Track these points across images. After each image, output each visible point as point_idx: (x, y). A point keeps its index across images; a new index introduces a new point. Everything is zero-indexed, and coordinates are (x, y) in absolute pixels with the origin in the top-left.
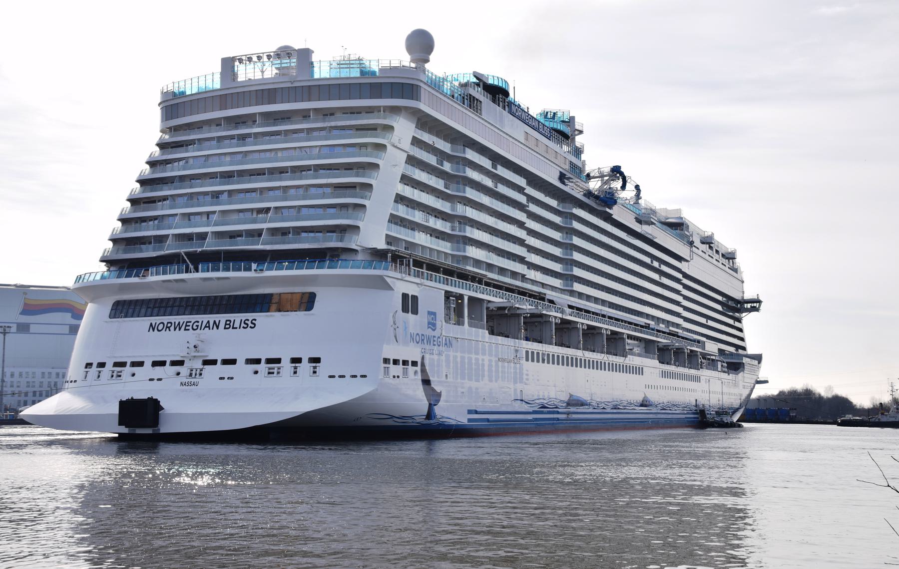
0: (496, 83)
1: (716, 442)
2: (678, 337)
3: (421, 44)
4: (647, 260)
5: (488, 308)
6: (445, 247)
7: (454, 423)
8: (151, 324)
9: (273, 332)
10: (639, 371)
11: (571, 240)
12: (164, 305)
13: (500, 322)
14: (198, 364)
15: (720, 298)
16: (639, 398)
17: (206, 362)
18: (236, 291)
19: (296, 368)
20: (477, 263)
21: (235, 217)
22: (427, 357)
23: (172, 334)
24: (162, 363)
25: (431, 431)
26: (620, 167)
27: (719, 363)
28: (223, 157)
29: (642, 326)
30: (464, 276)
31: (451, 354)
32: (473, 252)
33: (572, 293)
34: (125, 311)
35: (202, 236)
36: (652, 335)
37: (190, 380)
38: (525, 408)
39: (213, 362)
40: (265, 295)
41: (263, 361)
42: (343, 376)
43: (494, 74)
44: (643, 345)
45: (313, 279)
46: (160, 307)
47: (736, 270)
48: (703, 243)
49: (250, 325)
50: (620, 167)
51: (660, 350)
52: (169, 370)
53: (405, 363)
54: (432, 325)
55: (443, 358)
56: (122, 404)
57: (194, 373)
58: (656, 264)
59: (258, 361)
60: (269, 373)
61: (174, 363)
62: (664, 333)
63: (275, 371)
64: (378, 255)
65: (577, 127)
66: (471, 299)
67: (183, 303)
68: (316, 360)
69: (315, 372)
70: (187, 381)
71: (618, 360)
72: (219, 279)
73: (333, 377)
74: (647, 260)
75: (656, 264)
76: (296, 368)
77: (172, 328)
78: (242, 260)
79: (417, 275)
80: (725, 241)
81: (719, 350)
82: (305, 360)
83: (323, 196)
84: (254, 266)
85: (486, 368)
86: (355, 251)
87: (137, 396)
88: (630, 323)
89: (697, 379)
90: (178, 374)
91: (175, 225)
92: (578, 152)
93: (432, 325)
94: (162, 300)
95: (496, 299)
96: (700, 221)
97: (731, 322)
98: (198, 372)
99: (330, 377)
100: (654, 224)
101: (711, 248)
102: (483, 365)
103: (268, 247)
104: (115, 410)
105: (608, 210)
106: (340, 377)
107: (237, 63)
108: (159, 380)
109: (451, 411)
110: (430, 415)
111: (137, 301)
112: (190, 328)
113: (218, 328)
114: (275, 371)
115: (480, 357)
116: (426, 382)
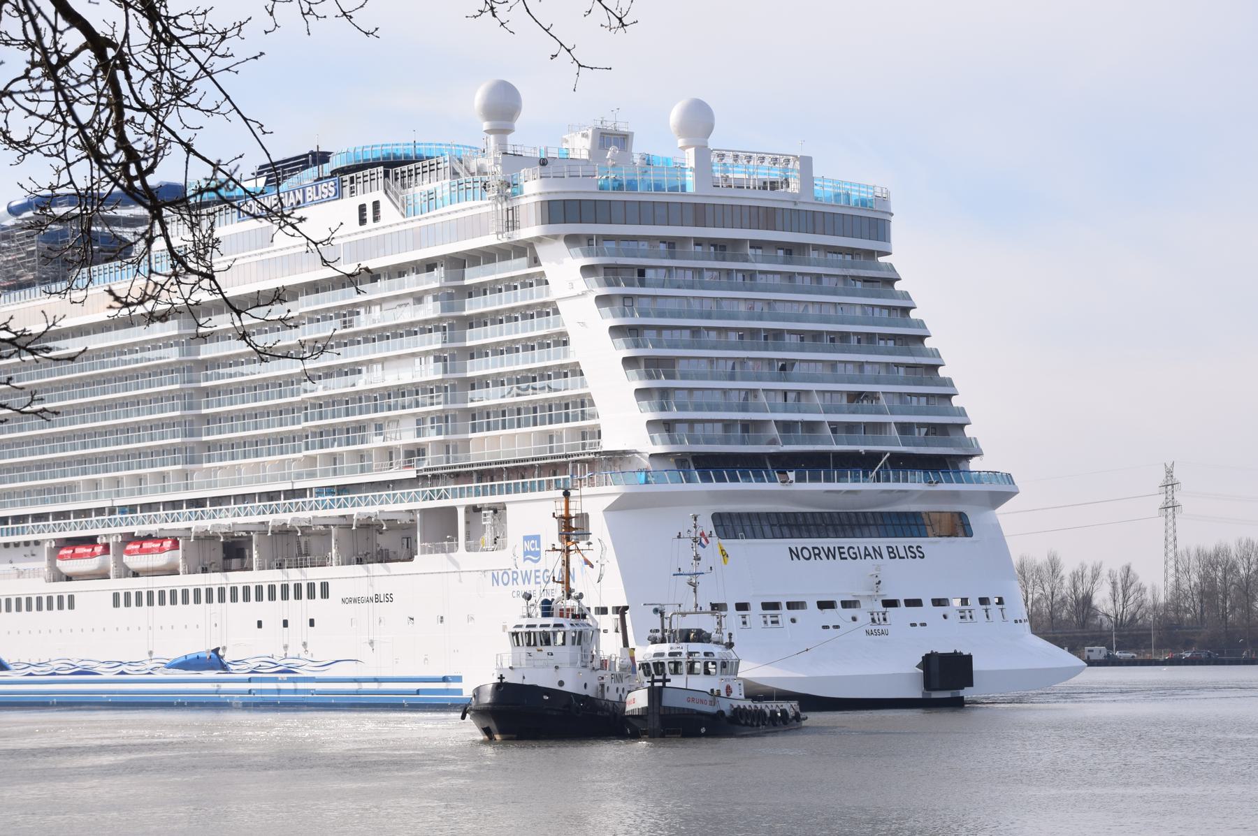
8: (791, 550)
18: (878, 506)
23: (823, 564)
34: (738, 529)
35: (811, 427)
45: (955, 495)
52: (838, 615)
56: (969, 657)
61: (845, 604)
63: (968, 614)
77: (822, 555)
94: (785, 514)
98: (881, 617)
111: (749, 515)
114: (968, 614)
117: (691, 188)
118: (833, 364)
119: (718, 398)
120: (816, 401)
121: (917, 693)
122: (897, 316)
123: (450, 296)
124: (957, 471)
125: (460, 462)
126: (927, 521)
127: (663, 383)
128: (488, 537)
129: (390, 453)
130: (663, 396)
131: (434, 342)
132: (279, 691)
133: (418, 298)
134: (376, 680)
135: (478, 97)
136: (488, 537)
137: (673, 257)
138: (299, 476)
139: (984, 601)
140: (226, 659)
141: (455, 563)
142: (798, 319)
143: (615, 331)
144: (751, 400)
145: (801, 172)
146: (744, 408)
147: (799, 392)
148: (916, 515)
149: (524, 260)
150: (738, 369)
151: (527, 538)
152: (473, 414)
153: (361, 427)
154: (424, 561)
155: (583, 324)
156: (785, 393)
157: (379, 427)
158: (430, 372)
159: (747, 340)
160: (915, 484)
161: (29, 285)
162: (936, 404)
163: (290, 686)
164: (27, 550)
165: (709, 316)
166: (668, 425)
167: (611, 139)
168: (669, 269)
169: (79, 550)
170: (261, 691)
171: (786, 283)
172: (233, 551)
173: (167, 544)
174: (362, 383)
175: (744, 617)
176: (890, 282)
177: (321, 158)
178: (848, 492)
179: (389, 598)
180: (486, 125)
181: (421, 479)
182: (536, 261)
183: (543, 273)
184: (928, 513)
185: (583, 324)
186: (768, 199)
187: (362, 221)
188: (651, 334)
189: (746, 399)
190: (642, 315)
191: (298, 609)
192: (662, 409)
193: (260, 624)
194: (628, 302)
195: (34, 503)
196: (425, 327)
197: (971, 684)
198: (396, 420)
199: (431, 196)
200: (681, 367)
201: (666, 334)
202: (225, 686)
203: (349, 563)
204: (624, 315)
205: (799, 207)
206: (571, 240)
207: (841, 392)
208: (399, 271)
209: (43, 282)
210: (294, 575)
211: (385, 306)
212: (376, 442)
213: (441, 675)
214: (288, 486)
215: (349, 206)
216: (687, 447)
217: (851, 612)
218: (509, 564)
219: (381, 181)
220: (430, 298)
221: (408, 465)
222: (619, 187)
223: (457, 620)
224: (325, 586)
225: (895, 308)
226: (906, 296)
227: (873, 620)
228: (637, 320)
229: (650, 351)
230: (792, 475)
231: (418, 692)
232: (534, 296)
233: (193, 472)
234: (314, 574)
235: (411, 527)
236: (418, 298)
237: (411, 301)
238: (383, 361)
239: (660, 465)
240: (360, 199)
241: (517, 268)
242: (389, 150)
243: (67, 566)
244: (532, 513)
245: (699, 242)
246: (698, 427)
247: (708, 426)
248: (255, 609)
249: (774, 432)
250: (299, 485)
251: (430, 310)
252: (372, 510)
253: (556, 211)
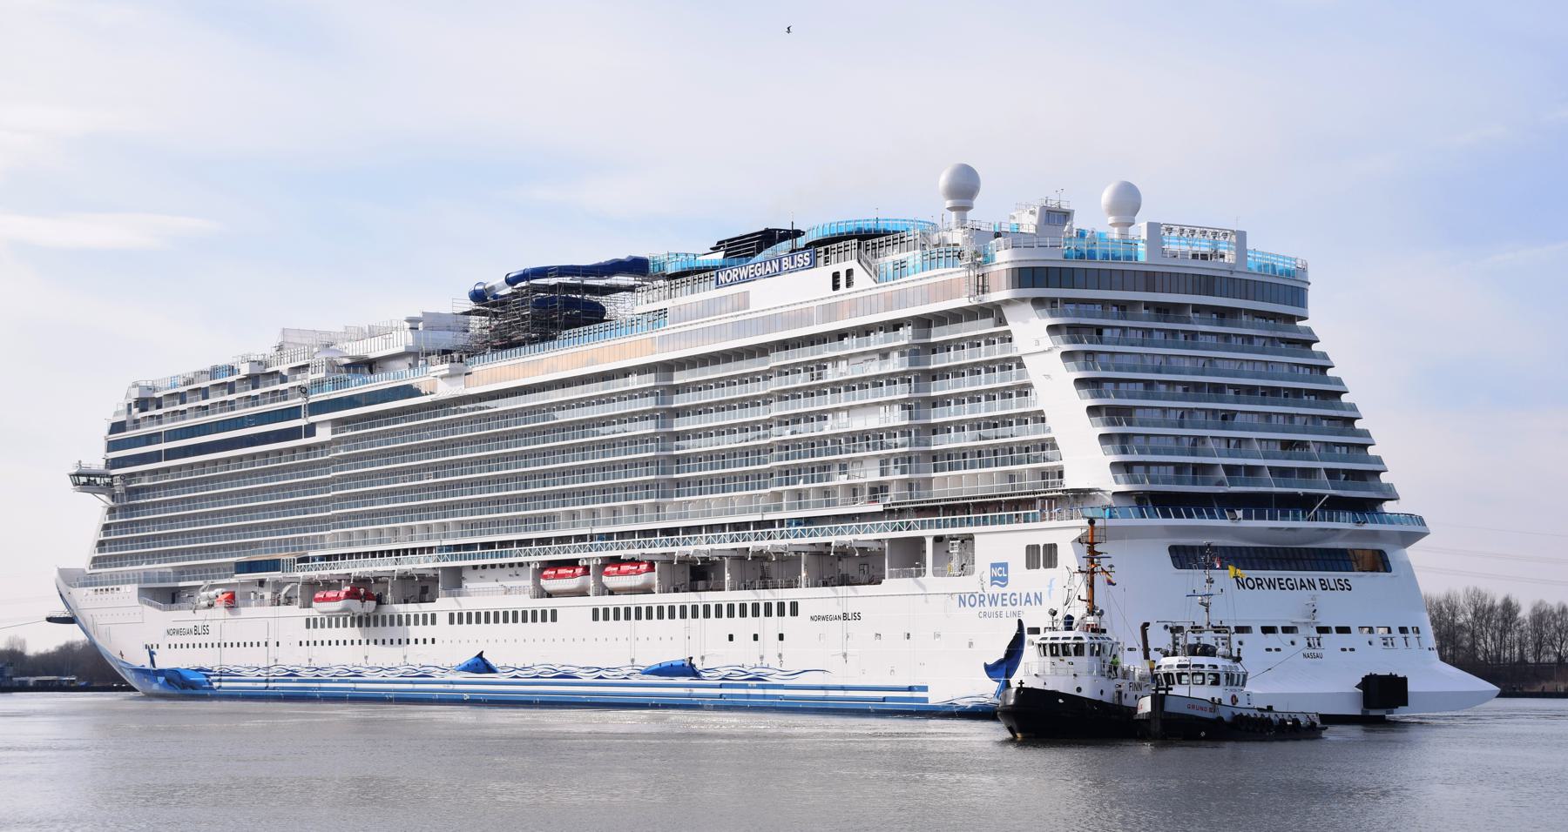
14: (1315, 634)
17: (1323, 630)
35: (1252, 471)
45: (1375, 534)
56: (1405, 680)
61: (1286, 630)
117: (1142, 258)
118: (1268, 415)
119: (1171, 443)
120: (1254, 446)
121: (1356, 710)
122: (1316, 373)
123: (917, 352)
124: (1374, 511)
125: (923, 498)
127: (1124, 429)
128: (955, 564)
129: (854, 490)
130: (1122, 442)
131: (901, 392)
132: (748, 696)
133: (884, 354)
134: (843, 688)
135: (943, 180)
136: (955, 564)
137: (1125, 318)
138: (767, 509)
139: (1403, 630)
140: (699, 667)
141: (922, 586)
142: (1236, 375)
143: (1079, 382)
144: (1199, 446)
145: (1237, 244)
146: (1194, 454)
147: (1239, 440)
148: (1343, 551)
149: (991, 320)
150: (1186, 418)
151: (994, 566)
152: (934, 456)
153: (825, 467)
154: (890, 584)
155: (1048, 376)
156: (1228, 440)
157: (843, 467)
158: (896, 418)
159: (1191, 393)
160: (1345, 524)
161: (520, 344)
162: (1353, 452)
163: (760, 692)
164: (512, 571)
165: (1159, 371)
166: (1127, 467)
167: (1055, 217)
168: (1124, 329)
169: (561, 571)
170: (732, 696)
171: (1221, 342)
172: (700, 574)
173: (644, 567)
174: (829, 428)
176: (1308, 344)
177: (798, 233)
179: (857, 616)
180: (949, 203)
181: (889, 513)
182: (1001, 321)
183: (1009, 332)
184: (1353, 550)
185: (1048, 376)
186: (1200, 268)
187: (836, 287)
188: (1109, 386)
189: (1195, 444)
190: (1104, 369)
191: (773, 624)
192: (1124, 452)
193: (731, 638)
194: (1090, 358)
195: (518, 530)
196: (891, 379)
197: (1405, 703)
198: (860, 461)
199: (901, 266)
200: (1138, 415)
201: (1123, 386)
202: (696, 691)
203: (816, 585)
204: (1087, 368)
205: (1235, 276)
206: (1038, 302)
208: (866, 331)
209: (532, 341)
210: (764, 596)
211: (851, 361)
212: (842, 480)
213: (907, 684)
214: (758, 518)
215: (824, 273)
216: (1147, 486)
217: (1290, 637)
218: (977, 588)
219: (855, 252)
220: (896, 354)
221: (874, 500)
222: (1082, 256)
223: (936, 634)
224: (794, 606)
225: (1316, 367)
226: (1324, 356)
228: (1099, 374)
229: (1113, 401)
230: (1240, 513)
231: (884, 699)
232: (998, 352)
233: (664, 505)
234: (786, 595)
235: (880, 554)
236: (884, 354)
237: (877, 356)
238: (848, 409)
239: (1121, 503)
240: (833, 268)
241: (984, 327)
242: (860, 225)
243: (549, 585)
244: (1000, 543)
245: (1148, 305)
246: (1153, 469)
247: (1162, 468)
248: (727, 624)
249: (1222, 474)
250: (768, 517)
251: (895, 364)
252: (847, 538)
253: (1025, 277)
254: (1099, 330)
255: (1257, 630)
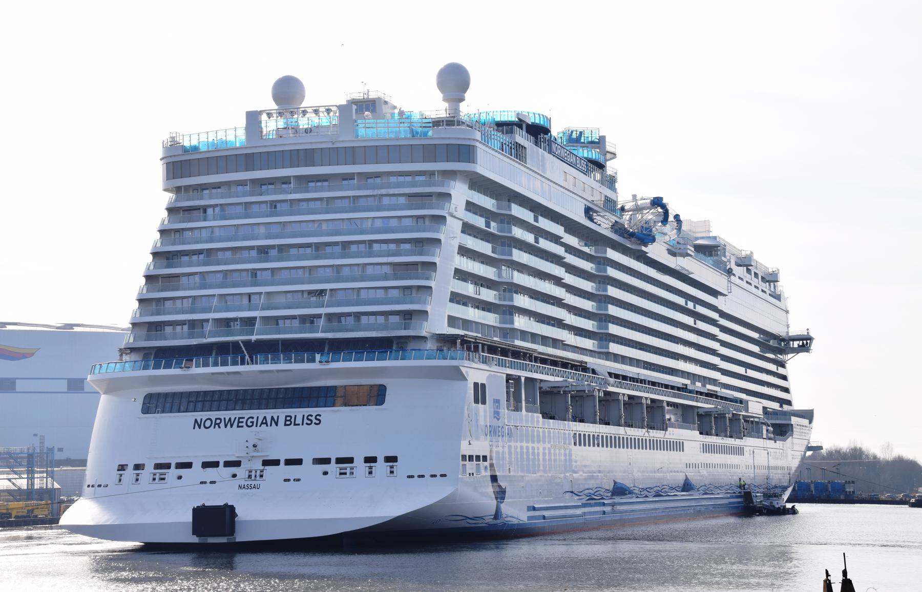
0: (537, 121)
1: (764, 533)
2: (717, 397)
3: (454, 80)
4: (680, 301)
5: (540, 388)
6: (491, 319)
7: (516, 522)
8: (196, 421)
9: (341, 429)
10: (678, 446)
11: (606, 290)
12: (208, 398)
13: (552, 403)
15: (755, 335)
16: (680, 479)
17: (266, 463)
19: (371, 468)
20: (524, 335)
21: (282, 300)
22: (494, 449)
24: (215, 464)
25: (492, 534)
26: (662, 198)
27: (764, 427)
28: (256, 227)
29: (679, 389)
30: (517, 354)
31: (513, 444)
32: (520, 322)
33: (608, 356)
34: (160, 405)
35: (251, 322)
36: (692, 399)
37: (249, 483)
38: (575, 501)
39: (276, 463)
40: (328, 388)
41: (333, 461)
42: (423, 476)
43: (533, 112)
44: (680, 412)
46: (204, 401)
47: (778, 297)
48: (738, 265)
49: (314, 421)
50: (662, 198)
51: (700, 416)
53: (478, 458)
54: (497, 415)
55: (506, 449)
57: (253, 474)
58: (690, 305)
59: (327, 461)
60: (341, 474)
61: (228, 464)
62: (701, 393)
63: (348, 471)
64: (448, 341)
65: (608, 148)
66: (526, 378)
67: (232, 397)
68: (391, 459)
69: (392, 472)
70: (246, 483)
71: (656, 434)
72: (278, 371)
73: (412, 477)
74: (680, 301)
75: (690, 305)
76: (371, 468)
77: (222, 425)
78: (307, 350)
79: (485, 361)
80: (765, 260)
81: (765, 408)
82: (381, 460)
83: (386, 278)
84: (318, 357)
85: (541, 457)
86: (424, 338)
87: (208, 503)
88: (667, 386)
89: (740, 451)
90: (234, 476)
91: (212, 305)
92: (611, 182)
93: (497, 415)
94: (206, 393)
95: (550, 377)
96: (736, 237)
97: (772, 367)
98: (258, 473)
99: (409, 477)
100: (689, 255)
101: (749, 271)
102: (538, 454)
103: (330, 335)
104: (189, 518)
105: (644, 248)
106: (419, 476)
107: (264, 117)
108: (213, 482)
109: (515, 512)
110: (497, 515)
112: (244, 424)
113: (277, 424)
114: (348, 471)
115: (536, 445)
116: (494, 478)
121: (195, 540)
126: (340, 393)
148: (328, 389)
156: (250, 295)
175: (138, 475)
178: (229, 373)
194: (177, 235)
207: (303, 291)
217: (234, 470)
227: (250, 476)
254: (204, 209)
255: (197, 465)
